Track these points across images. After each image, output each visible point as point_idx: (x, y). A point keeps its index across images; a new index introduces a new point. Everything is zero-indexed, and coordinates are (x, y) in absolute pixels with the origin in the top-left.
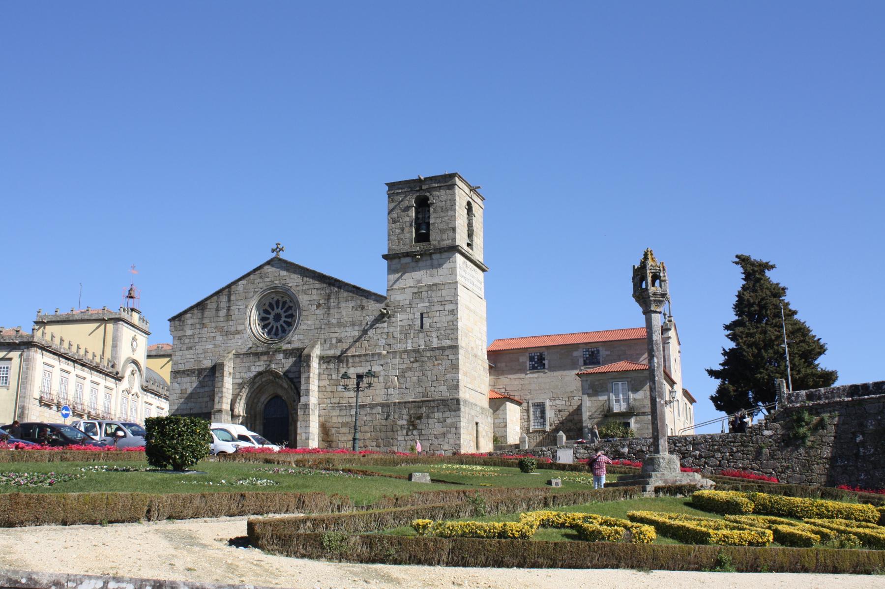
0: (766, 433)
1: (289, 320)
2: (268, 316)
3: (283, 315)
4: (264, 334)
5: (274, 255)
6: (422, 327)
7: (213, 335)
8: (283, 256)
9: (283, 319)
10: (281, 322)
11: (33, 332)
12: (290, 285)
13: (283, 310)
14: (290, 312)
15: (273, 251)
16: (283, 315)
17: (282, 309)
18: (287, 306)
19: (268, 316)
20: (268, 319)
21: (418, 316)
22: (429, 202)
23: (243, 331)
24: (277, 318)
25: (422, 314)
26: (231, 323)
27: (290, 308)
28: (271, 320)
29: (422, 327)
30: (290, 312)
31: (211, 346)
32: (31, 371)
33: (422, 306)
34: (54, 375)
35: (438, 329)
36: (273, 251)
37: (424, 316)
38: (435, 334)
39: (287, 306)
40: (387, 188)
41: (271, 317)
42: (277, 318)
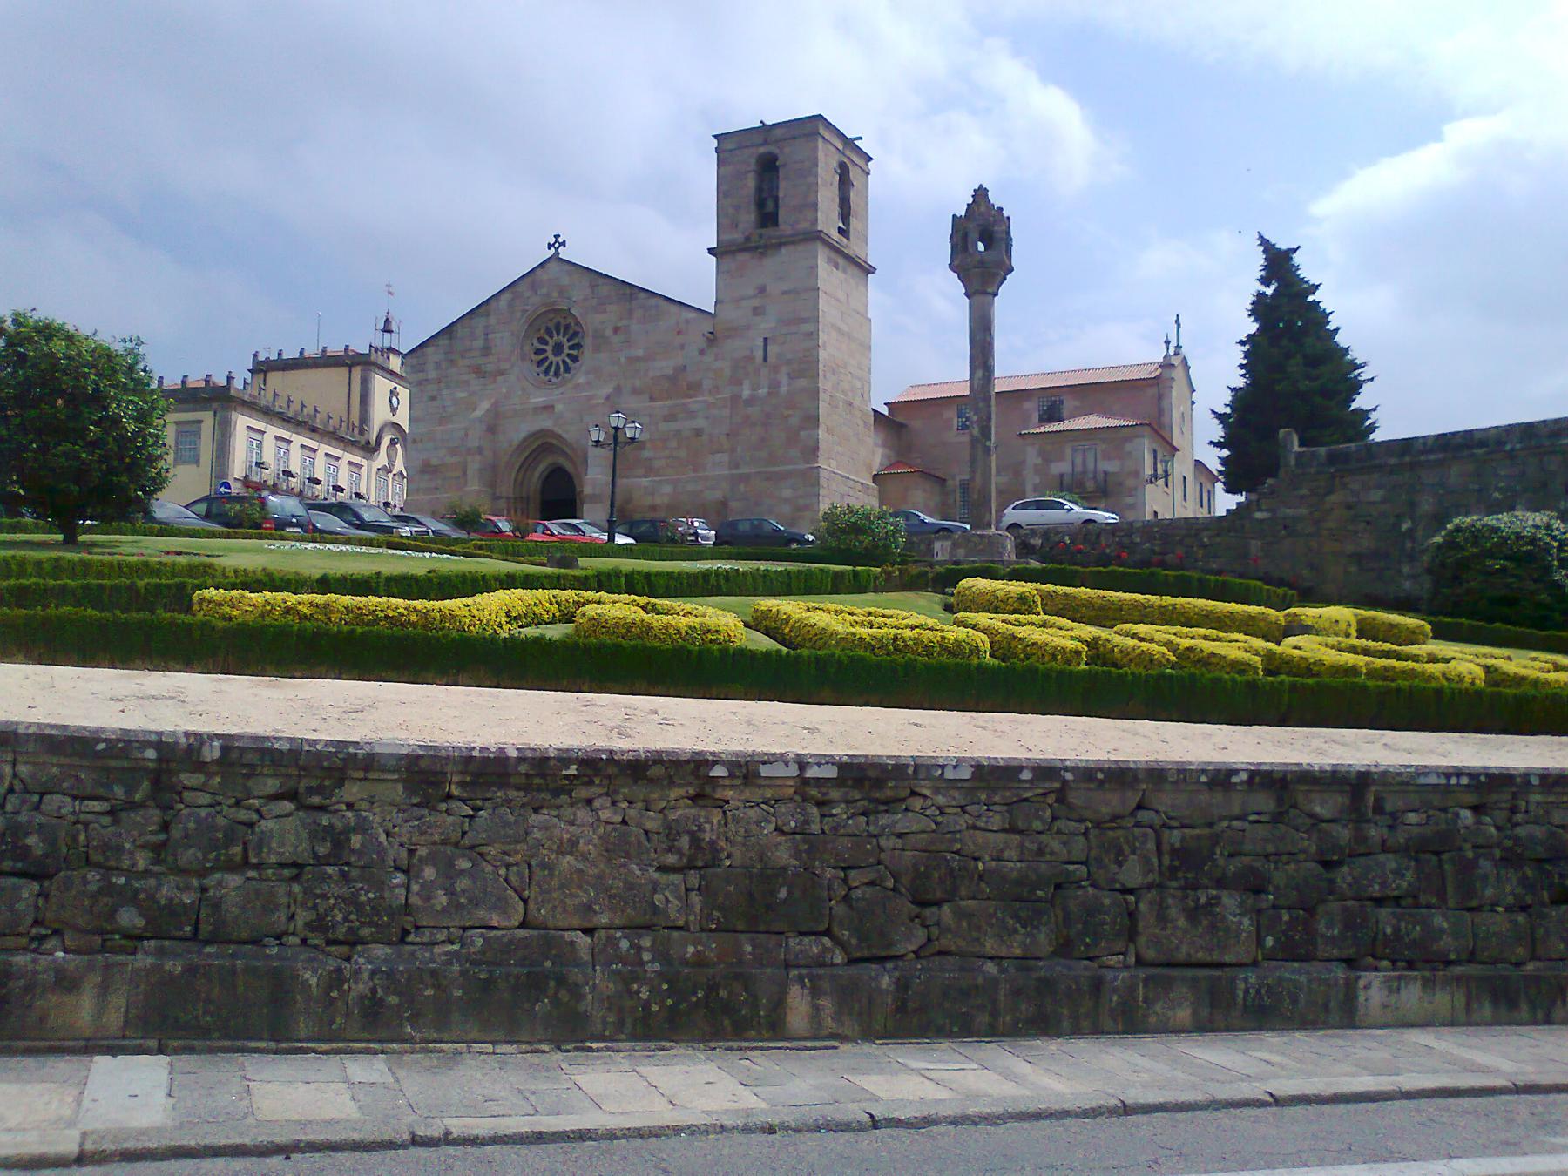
0: (1258, 515)
1: (574, 352)
2: (544, 347)
6: (765, 359)
7: (465, 377)
8: (564, 253)
9: (566, 351)
10: (564, 356)
13: (567, 337)
14: (575, 341)
15: (550, 246)
16: (566, 345)
18: (571, 331)
19: (544, 347)
20: (544, 351)
21: (760, 343)
22: (777, 163)
24: (558, 349)
25: (766, 339)
26: (492, 359)
27: (576, 334)
28: (549, 354)
29: (765, 359)
30: (575, 341)
31: (463, 395)
33: (765, 325)
34: (265, 444)
35: (789, 362)
36: (550, 246)
38: (784, 370)
39: (571, 331)
40: (715, 143)
41: (549, 348)
42: (558, 349)
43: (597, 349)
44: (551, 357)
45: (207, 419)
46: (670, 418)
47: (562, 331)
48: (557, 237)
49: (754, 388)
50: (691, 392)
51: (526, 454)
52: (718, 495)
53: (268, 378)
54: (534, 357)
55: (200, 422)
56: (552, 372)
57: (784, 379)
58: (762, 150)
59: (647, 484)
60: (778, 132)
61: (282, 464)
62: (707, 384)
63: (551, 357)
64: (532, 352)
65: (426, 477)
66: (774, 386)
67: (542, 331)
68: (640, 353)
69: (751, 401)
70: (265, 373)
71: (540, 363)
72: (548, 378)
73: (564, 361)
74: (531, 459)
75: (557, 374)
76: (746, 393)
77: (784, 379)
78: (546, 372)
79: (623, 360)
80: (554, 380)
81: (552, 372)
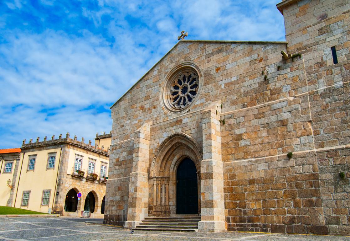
3: (189, 86)
4: (174, 106)
9: (189, 89)
10: (188, 93)
11: (67, 137)
13: (188, 83)
16: (189, 86)
17: (187, 83)
18: (191, 78)
21: (329, 51)
23: (158, 106)
24: (184, 90)
25: (334, 49)
27: (194, 79)
32: (65, 159)
33: (332, 40)
37: (336, 49)
39: (191, 78)
41: (180, 91)
43: (206, 83)
44: (181, 95)
45: (58, 150)
47: (186, 79)
50: (275, 96)
51: (166, 151)
52: (309, 169)
53: (100, 142)
54: (171, 97)
55: (56, 153)
59: (246, 164)
61: (78, 167)
63: (181, 95)
65: (117, 167)
67: (176, 82)
68: (234, 79)
70: (99, 139)
71: (175, 99)
73: (188, 96)
74: (170, 153)
75: (184, 104)
76: (322, 88)
78: (178, 104)
79: (223, 86)
80: (182, 107)
81: (181, 103)
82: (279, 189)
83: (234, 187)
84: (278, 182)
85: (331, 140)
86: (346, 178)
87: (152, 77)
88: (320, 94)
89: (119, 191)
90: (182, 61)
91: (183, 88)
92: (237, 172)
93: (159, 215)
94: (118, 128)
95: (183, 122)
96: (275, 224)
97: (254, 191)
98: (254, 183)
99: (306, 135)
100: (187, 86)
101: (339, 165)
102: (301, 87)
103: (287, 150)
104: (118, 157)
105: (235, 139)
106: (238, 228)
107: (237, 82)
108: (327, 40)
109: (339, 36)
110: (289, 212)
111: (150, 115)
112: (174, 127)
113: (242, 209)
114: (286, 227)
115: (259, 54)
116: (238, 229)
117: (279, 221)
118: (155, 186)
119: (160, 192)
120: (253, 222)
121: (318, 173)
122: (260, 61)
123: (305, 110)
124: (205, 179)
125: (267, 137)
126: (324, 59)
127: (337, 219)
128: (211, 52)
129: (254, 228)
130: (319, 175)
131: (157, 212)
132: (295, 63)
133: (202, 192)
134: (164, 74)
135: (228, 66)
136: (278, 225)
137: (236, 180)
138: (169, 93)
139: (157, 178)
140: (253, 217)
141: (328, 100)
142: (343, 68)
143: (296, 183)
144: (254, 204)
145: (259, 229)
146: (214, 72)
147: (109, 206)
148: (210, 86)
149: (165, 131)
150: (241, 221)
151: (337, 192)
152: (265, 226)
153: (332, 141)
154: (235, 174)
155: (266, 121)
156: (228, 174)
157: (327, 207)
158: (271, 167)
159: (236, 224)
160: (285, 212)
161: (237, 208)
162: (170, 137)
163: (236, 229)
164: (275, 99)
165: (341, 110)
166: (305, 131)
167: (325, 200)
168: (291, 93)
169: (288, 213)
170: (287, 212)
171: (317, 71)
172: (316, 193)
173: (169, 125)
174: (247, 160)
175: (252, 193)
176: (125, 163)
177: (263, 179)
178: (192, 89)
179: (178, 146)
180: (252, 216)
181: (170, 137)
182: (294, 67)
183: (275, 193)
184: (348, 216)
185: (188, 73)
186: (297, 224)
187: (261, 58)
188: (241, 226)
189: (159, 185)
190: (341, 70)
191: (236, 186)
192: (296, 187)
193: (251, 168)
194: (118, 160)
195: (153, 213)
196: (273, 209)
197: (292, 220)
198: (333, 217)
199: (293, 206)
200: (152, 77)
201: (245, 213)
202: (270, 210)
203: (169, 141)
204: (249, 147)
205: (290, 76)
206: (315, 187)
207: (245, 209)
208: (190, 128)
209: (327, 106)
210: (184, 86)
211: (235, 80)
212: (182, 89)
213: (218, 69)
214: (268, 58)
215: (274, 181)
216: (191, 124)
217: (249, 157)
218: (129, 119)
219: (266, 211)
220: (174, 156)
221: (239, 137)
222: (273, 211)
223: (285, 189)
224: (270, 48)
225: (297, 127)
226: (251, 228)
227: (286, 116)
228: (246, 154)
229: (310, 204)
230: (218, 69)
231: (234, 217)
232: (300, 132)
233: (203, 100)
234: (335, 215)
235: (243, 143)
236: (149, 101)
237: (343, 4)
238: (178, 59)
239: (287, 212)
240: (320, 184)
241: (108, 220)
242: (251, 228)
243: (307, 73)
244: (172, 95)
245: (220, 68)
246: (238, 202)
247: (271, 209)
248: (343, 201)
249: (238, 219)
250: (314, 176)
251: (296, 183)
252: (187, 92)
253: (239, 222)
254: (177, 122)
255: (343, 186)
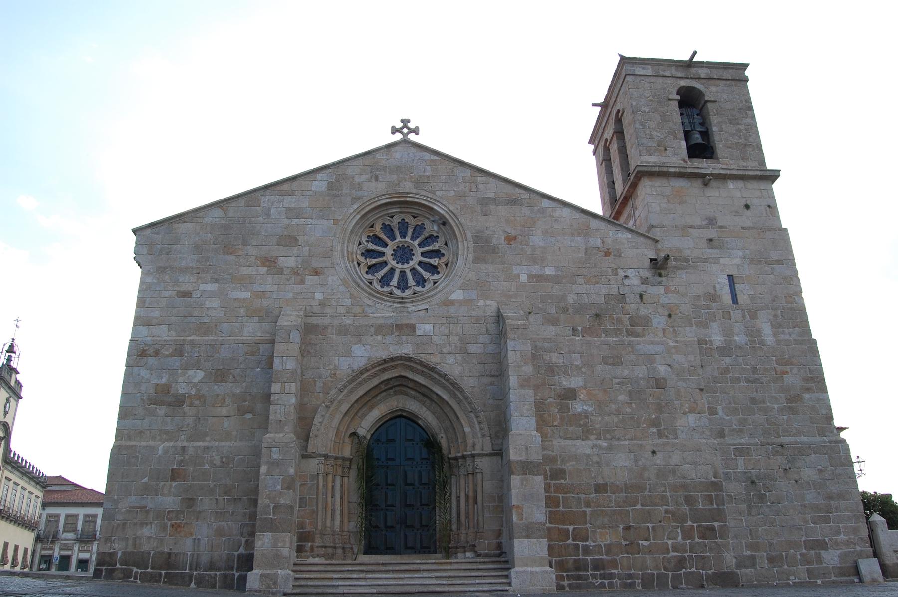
5: (398, 137)
7: (245, 271)
9: (417, 258)
12: (438, 193)
15: (394, 130)
24: (404, 254)
25: (730, 277)
42: (404, 254)
46: (616, 361)
48: (405, 122)
49: (728, 333)
50: (639, 329)
56: (394, 282)
57: (767, 330)
58: (683, 83)
59: (588, 451)
60: (703, 73)
62: (659, 321)
64: (359, 252)
65: (161, 411)
66: (754, 334)
68: (549, 271)
69: (724, 350)
72: (386, 289)
76: (718, 338)
77: (767, 330)
79: (524, 278)
80: (398, 292)
81: (394, 282)
82: (655, 505)
83: (561, 496)
84: (652, 493)
85: (735, 427)
86: (763, 492)
87: (308, 193)
88: (716, 346)
89: (173, 479)
90: (407, 186)
91: (398, 247)
92: (569, 466)
93: (332, 556)
94: (166, 294)
95: (418, 332)
96: (649, 571)
97: (605, 508)
98: (606, 491)
99: (697, 412)
100: (411, 248)
101: (752, 471)
102: (684, 325)
103: (666, 434)
104: (164, 380)
105: (559, 396)
106: (569, 584)
107: (556, 280)
108: (722, 261)
109: (737, 261)
110: (675, 549)
111: (298, 288)
112: (389, 339)
113: (581, 543)
114: (670, 576)
115: (604, 240)
116: (569, 585)
117: (657, 565)
118: (321, 478)
119: (330, 495)
120: (603, 569)
121: (722, 480)
122: (607, 254)
123: (693, 368)
124: (523, 474)
125: (627, 403)
126: (719, 292)
127: (753, 558)
128: (492, 195)
129: (606, 581)
130: (724, 483)
131: (325, 547)
132: (672, 281)
133: (514, 502)
134: (349, 199)
135: (537, 240)
136: (655, 572)
137: (566, 482)
138: (357, 251)
139: (326, 457)
140: (602, 558)
141: (728, 360)
142: (747, 314)
143: (686, 496)
144: (607, 532)
145: (616, 582)
146: (499, 240)
147: (124, 524)
148: (491, 268)
149: (360, 341)
150: (577, 569)
151: (751, 514)
152: (630, 576)
153: (736, 429)
154: (563, 469)
155: (626, 373)
156: (548, 468)
157: (737, 539)
158: (640, 463)
159: (567, 575)
160: (668, 549)
161: (570, 541)
162: (385, 361)
163: (566, 585)
164: (637, 335)
165: (748, 381)
166: (695, 406)
167: (733, 527)
168: (667, 332)
169: (673, 551)
170: (670, 549)
171: (708, 307)
172: (719, 515)
173: (373, 329)
174: (589, 442)
175: (602, 511)
176: (197, 403)
177: (625, 484)
178: (427, 260)
179: (400, 385)
180: (601, 557)
181: (385, 360)
182: (671, 287)
183: (648, 512)
184: (767, 554)
185: (414, 217)
186: (689, 570)
187: (607, 249)
188: (579, 577)
189: (330, 477)
190: (744, 317)
191: (566, 494)
192: (686, 503)
193: (598, 460)
194: (165, 389)
195: (316, 551)
196: (645, 543)
197: (681, 562)
198: (747, 556)
199: (680, 538)
200: (308, 193)
201: (586, 550)
202: (638, 544)
203: (377, 368)
204: (592, 417)
205: (664, 300)
206: (718, 505)
207: (587, 543)
208: (441, 350)
209: (727, 370)
210: (400, 245)
211: (554, 273)
212: (394, 250)
213: (510, 239)
214: (623, 255)
215: (645, 489)
216: (443, 340)
217: (592, 437)
218: (216, 281)
219: (632, 547)
220: (372, 408)
221: (570, 394)
222: (646, 546)
223: (666, 505)
224: (624, 236)
225: (682, 396)
226: (600, 581)
227: (662, 370)
228: (586, 433)
229: (708, 532)
230: (510, 239)
231: (562, 560)
232: (687, 406)
233: (474, 295)
234: (749, 553)
235: (578, 407)
236: (295, 250)
237: (738, 213)
238: (395, 177)
239: (670, 549)
240: (725, 500)
241: (118, 566)
242: (600, 581)
243: (693, 304)
244: (362, 254)
245: (515, 238)
246: (571, 528)
247: (640, 542)
248: (760, 529)
249: (570, 565)
250: (716, 486)
251: (686, 496)
252: (411, 263)
253: (574, 571)
254: (399, 327)
255: (760, 505)
